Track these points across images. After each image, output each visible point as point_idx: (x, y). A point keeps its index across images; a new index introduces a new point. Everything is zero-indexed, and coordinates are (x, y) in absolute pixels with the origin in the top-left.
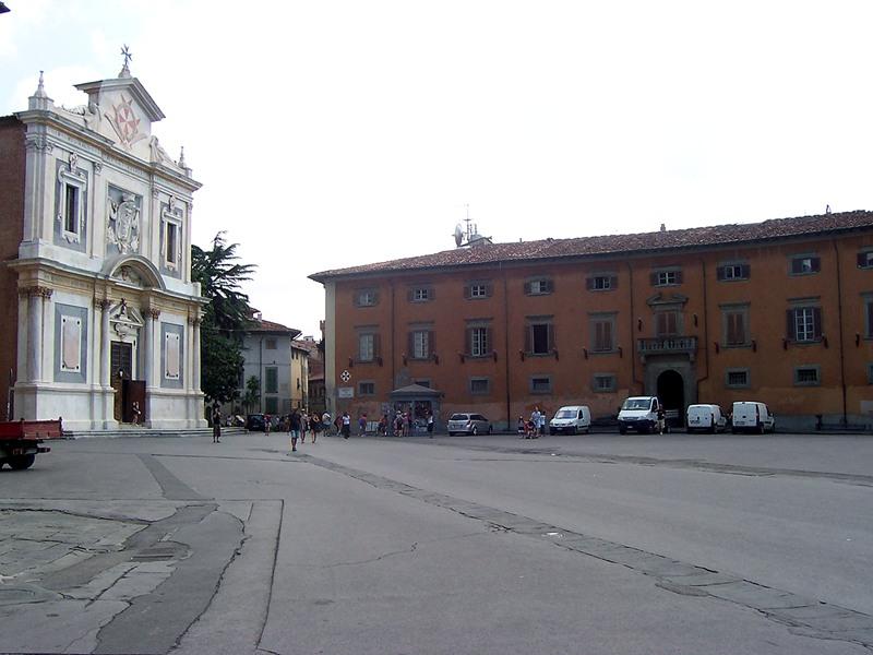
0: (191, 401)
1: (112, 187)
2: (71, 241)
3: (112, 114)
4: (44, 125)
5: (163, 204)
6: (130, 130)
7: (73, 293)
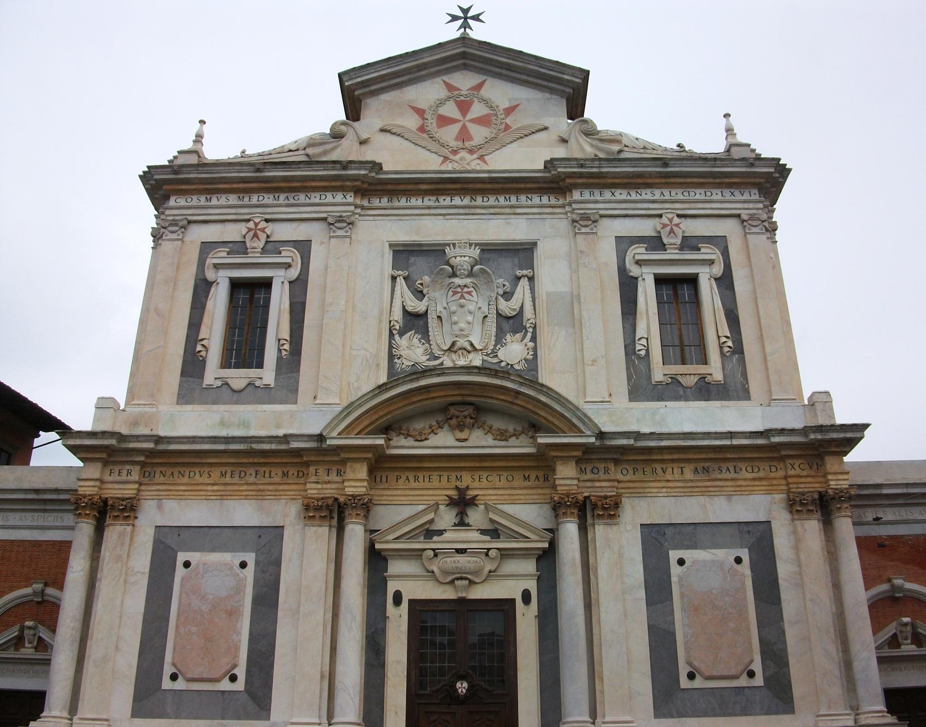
2: (238, 384)
6: (479, 134)
7: (222, 497)
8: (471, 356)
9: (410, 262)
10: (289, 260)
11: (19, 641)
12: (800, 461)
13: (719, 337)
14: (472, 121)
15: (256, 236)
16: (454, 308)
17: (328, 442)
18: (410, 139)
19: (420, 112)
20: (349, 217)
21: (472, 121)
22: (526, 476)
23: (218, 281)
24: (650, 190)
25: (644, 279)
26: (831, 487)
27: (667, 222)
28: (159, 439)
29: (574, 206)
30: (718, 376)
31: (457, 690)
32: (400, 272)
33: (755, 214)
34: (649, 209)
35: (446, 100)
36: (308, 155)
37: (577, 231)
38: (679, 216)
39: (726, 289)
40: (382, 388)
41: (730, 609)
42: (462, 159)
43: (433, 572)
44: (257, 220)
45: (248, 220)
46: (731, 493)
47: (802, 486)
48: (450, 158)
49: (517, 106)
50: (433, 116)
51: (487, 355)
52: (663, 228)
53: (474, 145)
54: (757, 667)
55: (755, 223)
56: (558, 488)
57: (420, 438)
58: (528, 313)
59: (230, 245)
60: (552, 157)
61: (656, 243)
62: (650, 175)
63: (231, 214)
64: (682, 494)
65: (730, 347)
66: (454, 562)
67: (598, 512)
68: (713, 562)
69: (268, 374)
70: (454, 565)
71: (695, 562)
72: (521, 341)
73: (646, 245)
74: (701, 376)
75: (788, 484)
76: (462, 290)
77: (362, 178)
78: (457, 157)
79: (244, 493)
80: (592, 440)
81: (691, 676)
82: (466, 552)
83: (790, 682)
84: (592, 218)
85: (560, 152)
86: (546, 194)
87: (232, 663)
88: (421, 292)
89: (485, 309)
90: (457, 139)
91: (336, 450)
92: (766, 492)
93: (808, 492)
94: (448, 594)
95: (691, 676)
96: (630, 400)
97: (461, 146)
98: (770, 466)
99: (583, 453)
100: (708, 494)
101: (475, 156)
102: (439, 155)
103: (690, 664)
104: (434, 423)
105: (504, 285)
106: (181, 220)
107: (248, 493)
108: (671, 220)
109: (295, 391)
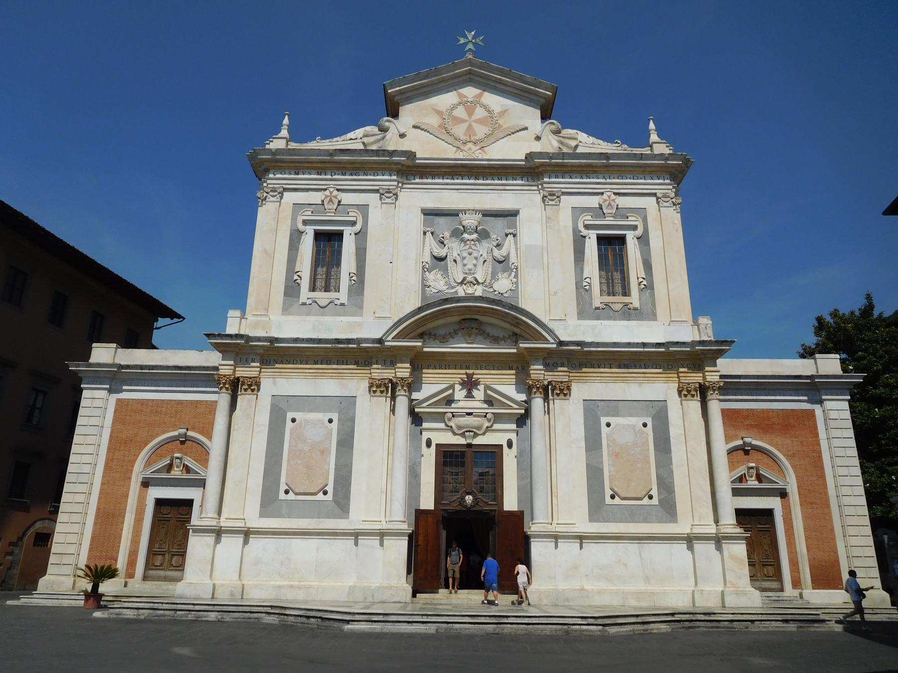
0: (706, 549)
1: (430, 213)
2: (323, 303)
3: (433, 121)
4: (267, 171)
5: (577, 211)
8: (475, 287)
9: (435, 222)
10: (354, 219)
11: (170, 467)
12: (687, 362)
13: (638, 278)
14: (475, 121)
15: (331, 201)
16: (465, 254)
17: (386, 343)
18: (434, 133)
19: (439, 113)
20: (394, 189)
21: (475, 121)
22: (511, 366)
23: (306, 232)
24: (596, 175)
25: (590, 238)
26: (707, 380)
27: (607, 198)
28: (273, 340)
29: (545, 185)
30: (636, 304)
31: (465, 501)
32: (428, 229)
33: (667, 193)
34: (595, 189)
35: (458, 105)
36: (364, 143)
37: (546, 203)
38: (615, 194)
39: (644, 245)
40: (420, 310)
41: (638, 456)
42: (470, 149)
43: (451, 427)
44: (331, 190)
45: (325, 190)
46: (642, 382)
47: (689, 378)
48: (461, 148)
49: (507, 110)
50: (449, 117)
51: (486, 286)
52: (604, 202)
53: (477, 139)
54: (654, 492)
55: (666, 200)
56: (532, 375)
57: (444, 339)
58: (513, 259)
59: (314, 206)
60: (531, 151)
61: (599, 211)
62: (597, 166)
63: (314, 184)
64: (610, 381)
65: (644, 285)
66: (465, 420)
67: (557, 392)
68: (629, 425)
69: (343, 296)
70: (465, 423)
71: (617, 425)
72: (508, 278)
73: (592, 214)
74: (625, 304)
75: (678, 377)
76: (470, 243)
77: (403, 163)
78: (466, 148)
79: (330, 375)
80: (555, 346)
81: (613, 497)
82: (472, 414)
83: (675, 503)
84: (556, 194)
85: (537, 147)
86: (525, 176)
87: (325, 483)
88: (443, 243)
89: (485, 255)
90: (465, 135)
91: (390, 348)
92: (665, 382)
93: (692, 383)
94: (461, 441)
95: (613, 497)
96: (578, 319)
97: (469, 140)
98: (668, 365)
99: (548, 354)
100: (627, 381)
101: (478, 147)
102: (453, 146)
103: (612, 489)
104: (452, 331)
105: (497, 240)
106: (279, 188)
107: (332, 375)
108: (609, 197)
109: (361, 307)
